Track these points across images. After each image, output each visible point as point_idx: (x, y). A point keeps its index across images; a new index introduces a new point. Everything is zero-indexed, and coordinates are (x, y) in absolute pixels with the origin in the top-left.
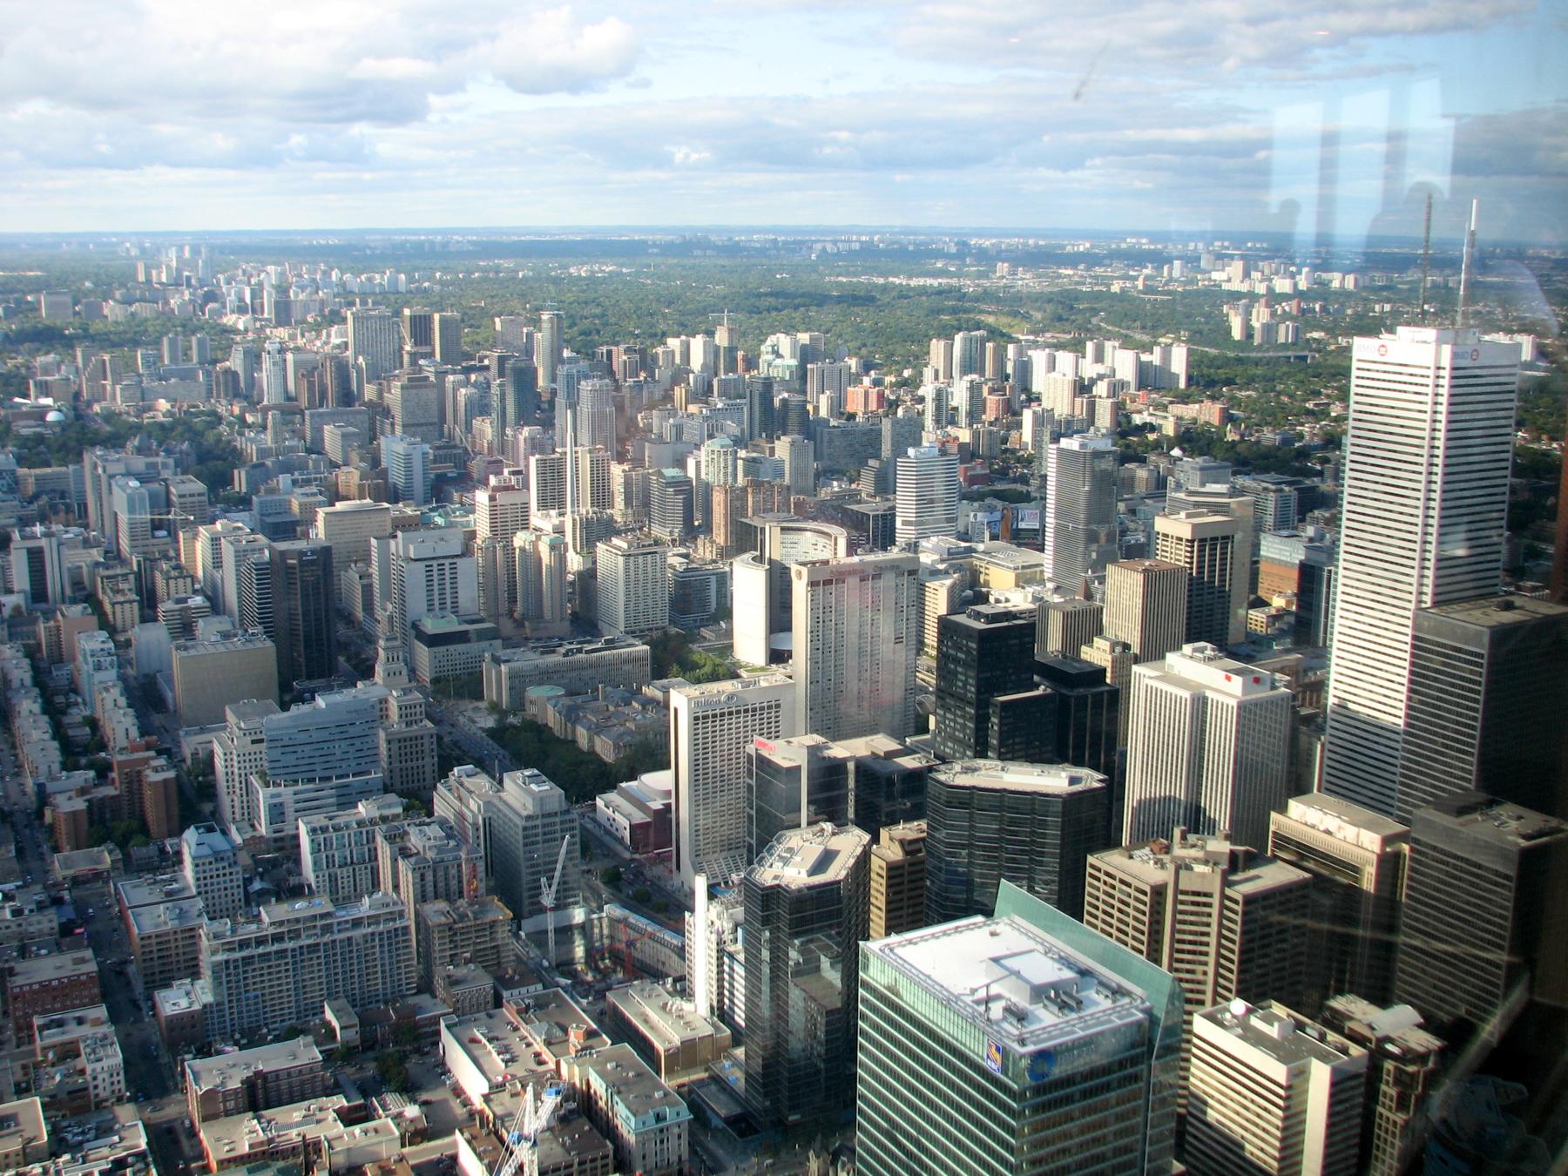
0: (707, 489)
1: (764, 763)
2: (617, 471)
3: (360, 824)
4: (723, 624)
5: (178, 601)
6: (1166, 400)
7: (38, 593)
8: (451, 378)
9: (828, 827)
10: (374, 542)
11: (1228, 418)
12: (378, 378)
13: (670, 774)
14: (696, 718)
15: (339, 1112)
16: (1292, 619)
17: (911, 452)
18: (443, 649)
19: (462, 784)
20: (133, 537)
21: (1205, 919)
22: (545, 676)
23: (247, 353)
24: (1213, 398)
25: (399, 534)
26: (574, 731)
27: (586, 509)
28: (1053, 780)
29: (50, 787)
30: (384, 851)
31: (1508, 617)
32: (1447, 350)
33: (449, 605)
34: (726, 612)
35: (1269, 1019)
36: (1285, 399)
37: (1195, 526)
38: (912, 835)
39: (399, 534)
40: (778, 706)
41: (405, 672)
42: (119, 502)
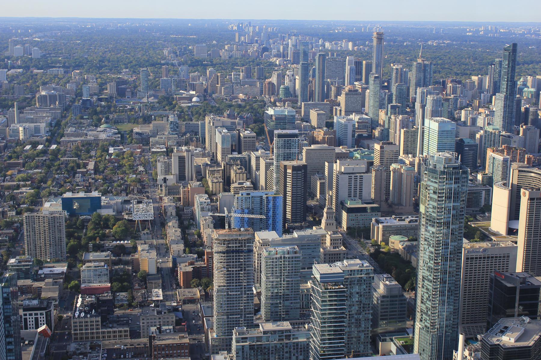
4: (487, 214)
5: (239, 184)
7: (182, 177)
9: (527, 319)
14: (467, 259)
18: (354, 214)
20: (223, 154)
22: (398, 231)
23: (278, 75)
25: (338, 161)
26: (410, 258)
29: (178, 260)
33: (358, 195)
34: (488, 208)
40: (508, 257)
41: (335, 224)
42: (218, 139)
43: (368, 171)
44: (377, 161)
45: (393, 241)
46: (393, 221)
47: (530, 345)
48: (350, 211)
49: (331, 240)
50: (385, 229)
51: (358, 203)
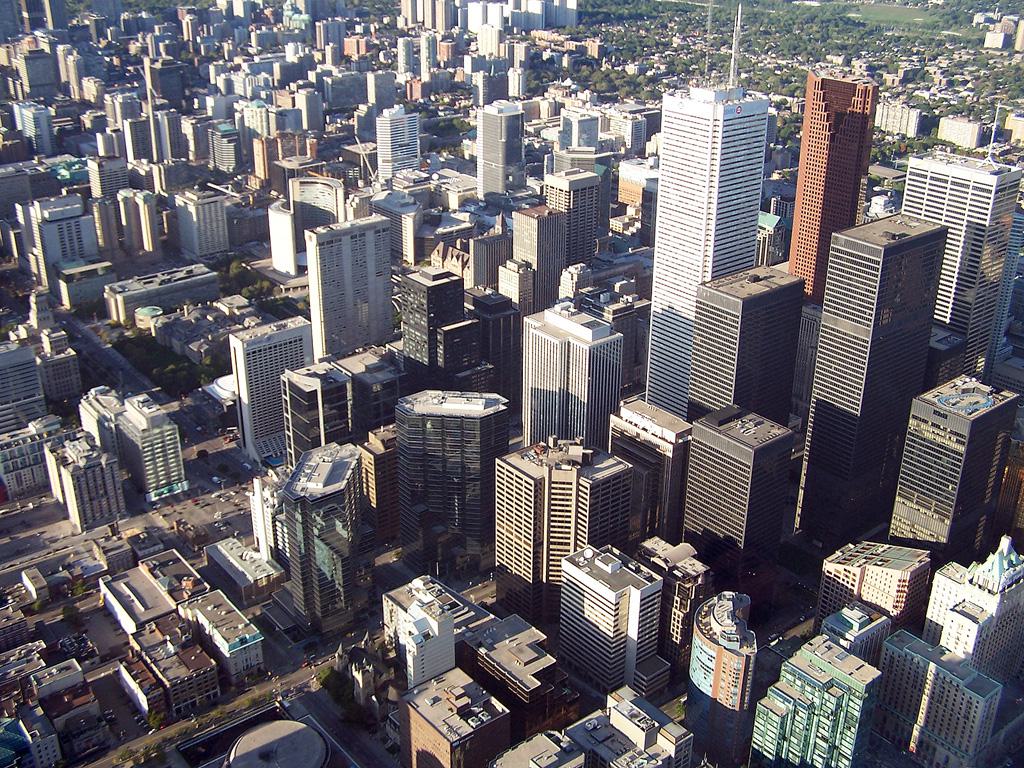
0: (253, 134)
1: (293, 386)
2: (187, 126)
3: (32, 438)
6: (562, 38)
8: (60, 48)
10: (18, 207)
11: (603, 52)
12: (7, 41)
13: (233, 377)
15: (43, 654)
16: (638, 225)
17: (385, 111)
19: (97, 400)
21: (568, 497)
24: (595, 35)
25: (36, 203)
26: (171, 343)
27: (169, 161)
28: (472, 406)
30: (51, 460)
31: (758, 289)
32: (720, 108)
35: (605, 561)
36: (643, 33)
37: (571, 183)
38: (391, 436)
39: (36, 203)
41: (51, 317)
43: (87, 211)
44: (97, 192)
45: (141, 317)
46: (135, 286)
47: (342, 488)
48: (69, 279)
49: (51, 343)
50: (127, 301)
51: (79, 265)
